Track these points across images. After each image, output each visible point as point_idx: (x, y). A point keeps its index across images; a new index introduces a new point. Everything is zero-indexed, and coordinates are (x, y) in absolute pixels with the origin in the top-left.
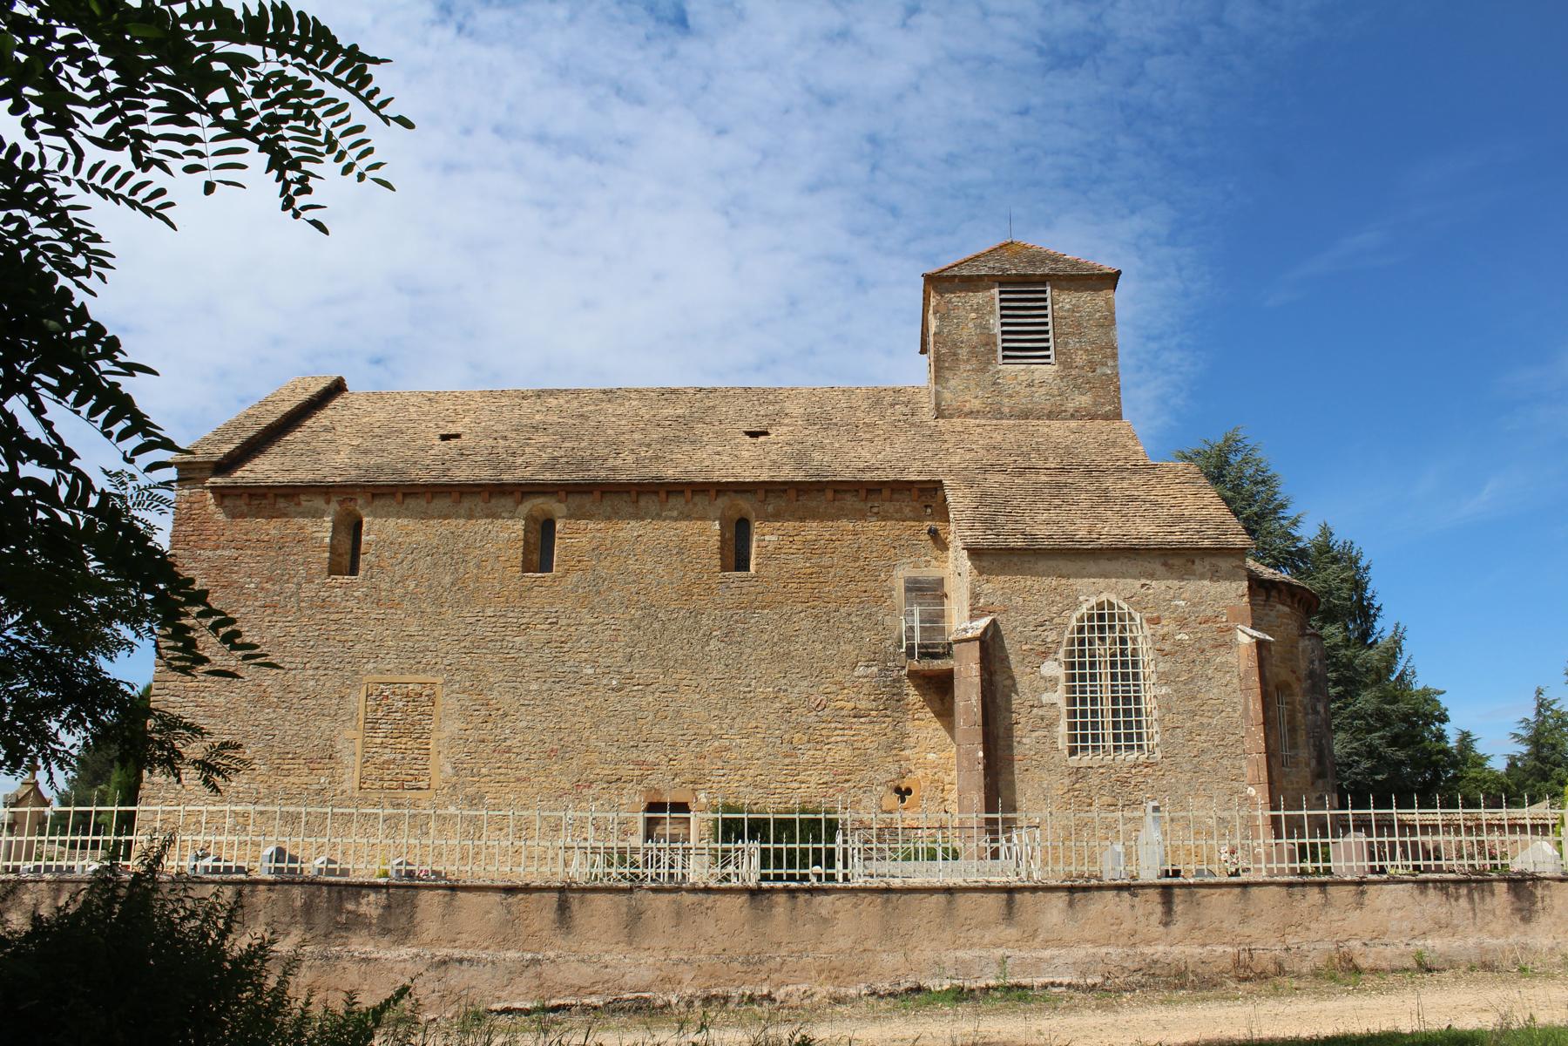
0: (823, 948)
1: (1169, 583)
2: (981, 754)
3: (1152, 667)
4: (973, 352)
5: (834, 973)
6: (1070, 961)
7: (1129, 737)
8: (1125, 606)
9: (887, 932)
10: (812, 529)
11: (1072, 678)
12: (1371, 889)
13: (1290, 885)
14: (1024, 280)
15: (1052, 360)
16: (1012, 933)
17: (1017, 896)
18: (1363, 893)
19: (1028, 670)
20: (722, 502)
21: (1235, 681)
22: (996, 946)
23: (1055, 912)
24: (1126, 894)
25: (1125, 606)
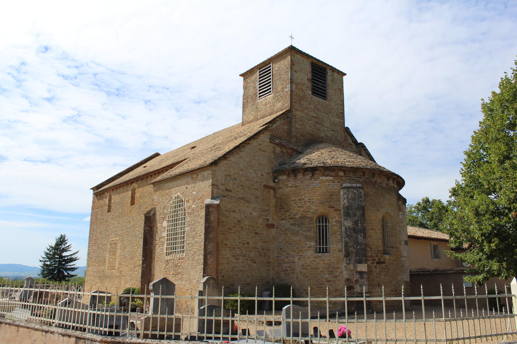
4: (252, 99)
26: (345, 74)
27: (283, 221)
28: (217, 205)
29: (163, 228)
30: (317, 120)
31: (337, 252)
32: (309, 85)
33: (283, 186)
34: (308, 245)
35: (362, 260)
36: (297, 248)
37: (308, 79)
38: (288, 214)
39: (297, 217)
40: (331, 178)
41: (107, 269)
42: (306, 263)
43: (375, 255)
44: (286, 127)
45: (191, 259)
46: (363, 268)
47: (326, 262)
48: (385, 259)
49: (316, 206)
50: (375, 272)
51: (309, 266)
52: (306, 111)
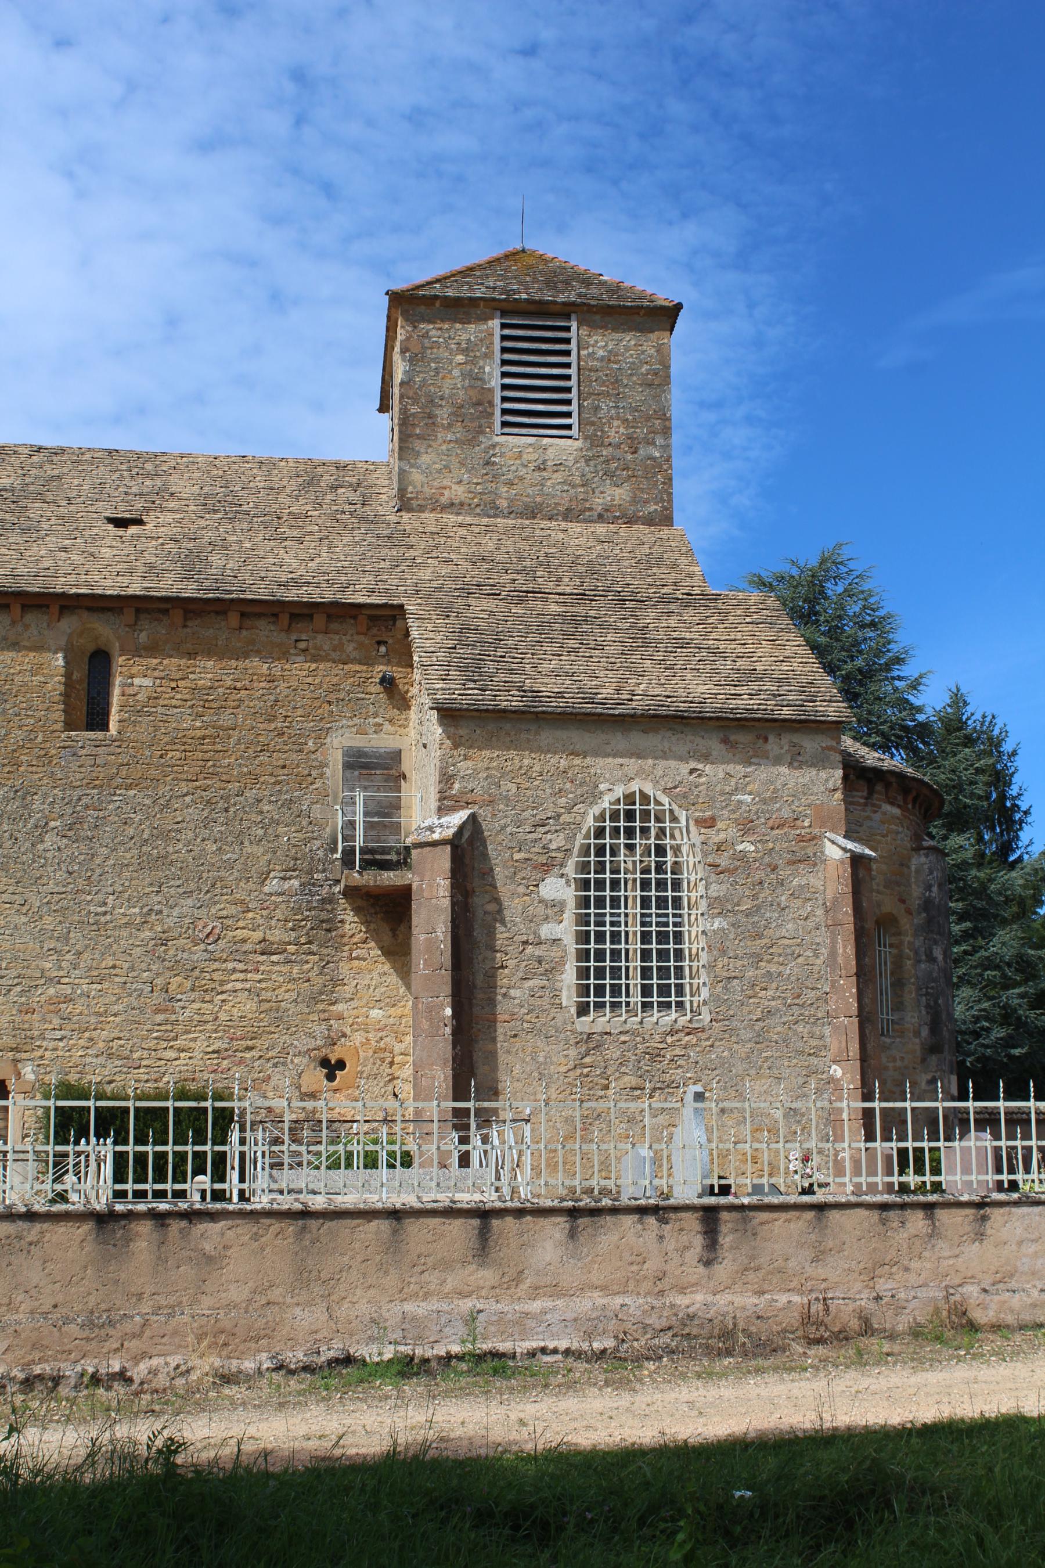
0: (206, 1301)
1: (730, 768)
2: (448, 1012)
3: (701, 890)
4: (458, 414)
5: (221, 1338)
6: (570, 1316)
7: (664, 991)
8: (665, 800)
9: (302, 1277)
10: (206, 670)
11: (585, 902)
12: (996, 1214)
13: (884, 1207)
14: (539, 309)
15: (574, 432)
16: (487, 1276)
17: (495, 1223)
18: (984, 1218)
19: (521, 889)
20: (68, 624)
21: (820, 912)
22: (462, 1295)
23: (549, 1245)
24: (651, 1220)
25: (665, 800)
47: (899, 1063)
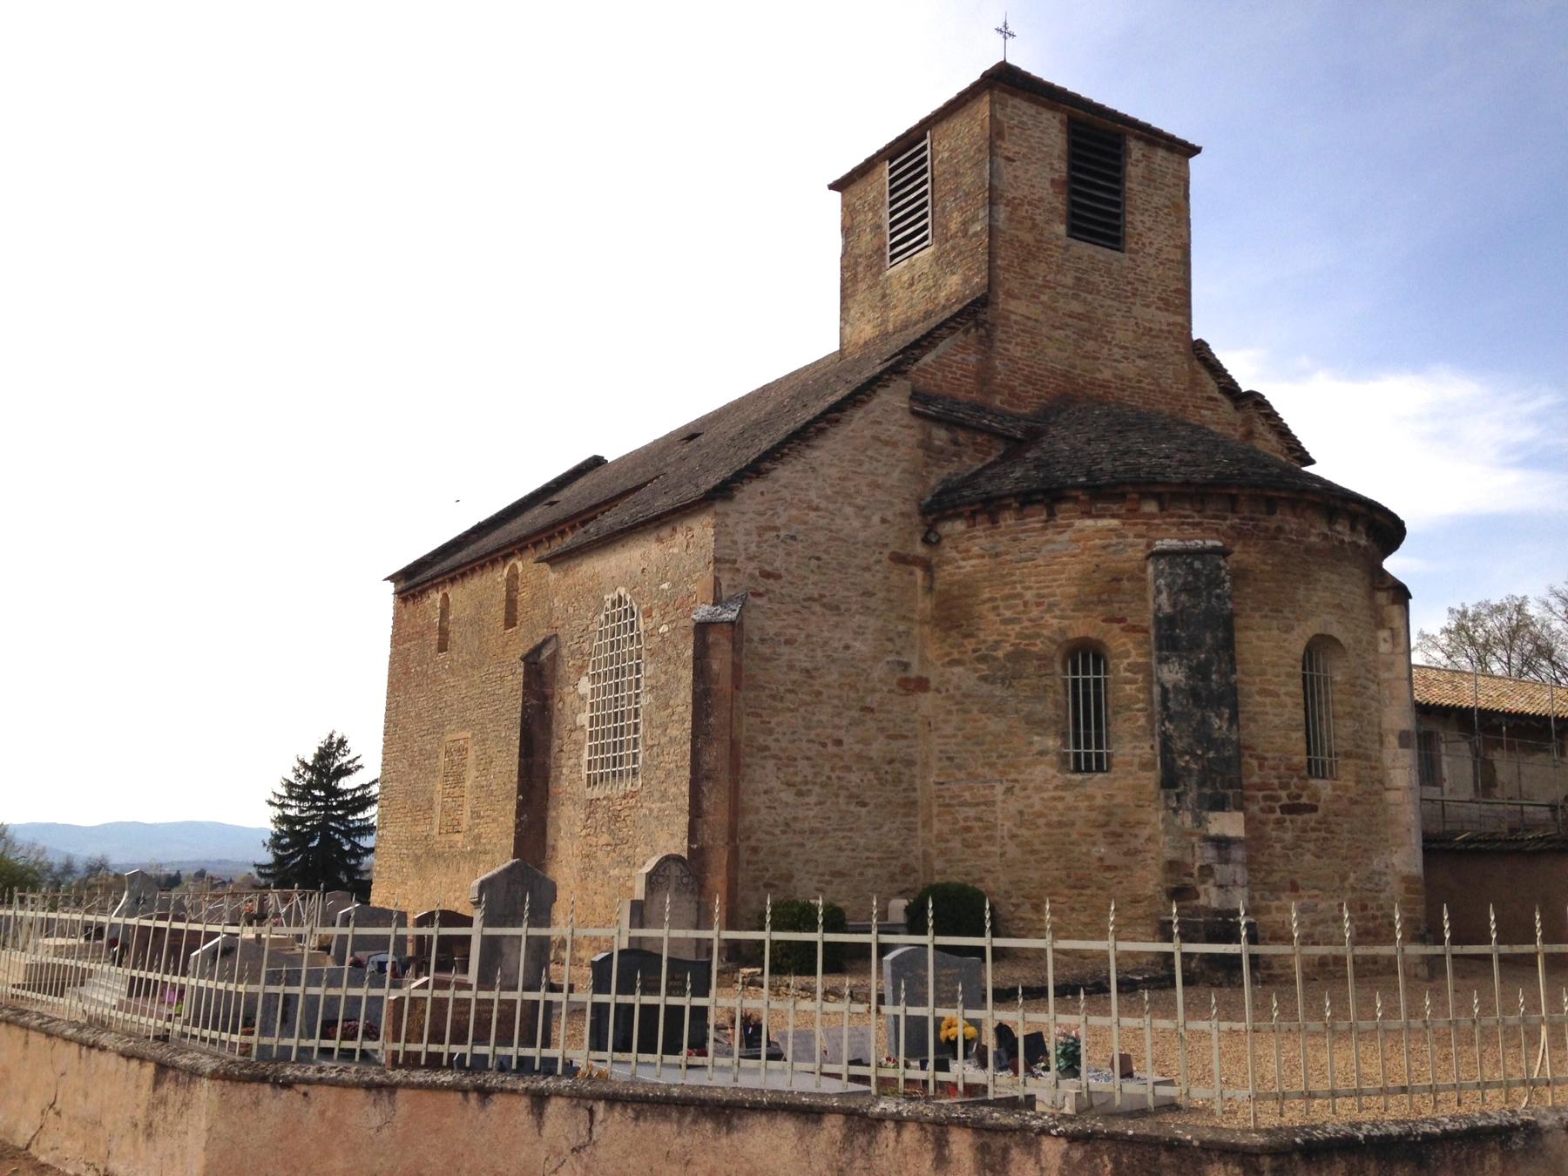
4: (869, 267)
26: (1195, 150)
27: (957, 670)
28: (732, 623)
29: (580, 698)
30: (1085, 325)
31: (1134, 768)
32: (1059, 203)
33: (954, 554)
34: (1036, 748)
35: (1225, 797)
36: (1000, 756)
37: (1053, 181)
38: (970, 644)
39: (1000, 654)
40: (1114, 523)
41: (436, 830)
42: (1032, 806)
43: (1276, 782)
44: (972, 359)
45: (657, 795)
46: (1229, 824)
47: (1099, 801)
48: (1315, 795)
49: (1062, 617)
50: (1280, 840)
51: (1040, 815)
52: (1044, 298)
